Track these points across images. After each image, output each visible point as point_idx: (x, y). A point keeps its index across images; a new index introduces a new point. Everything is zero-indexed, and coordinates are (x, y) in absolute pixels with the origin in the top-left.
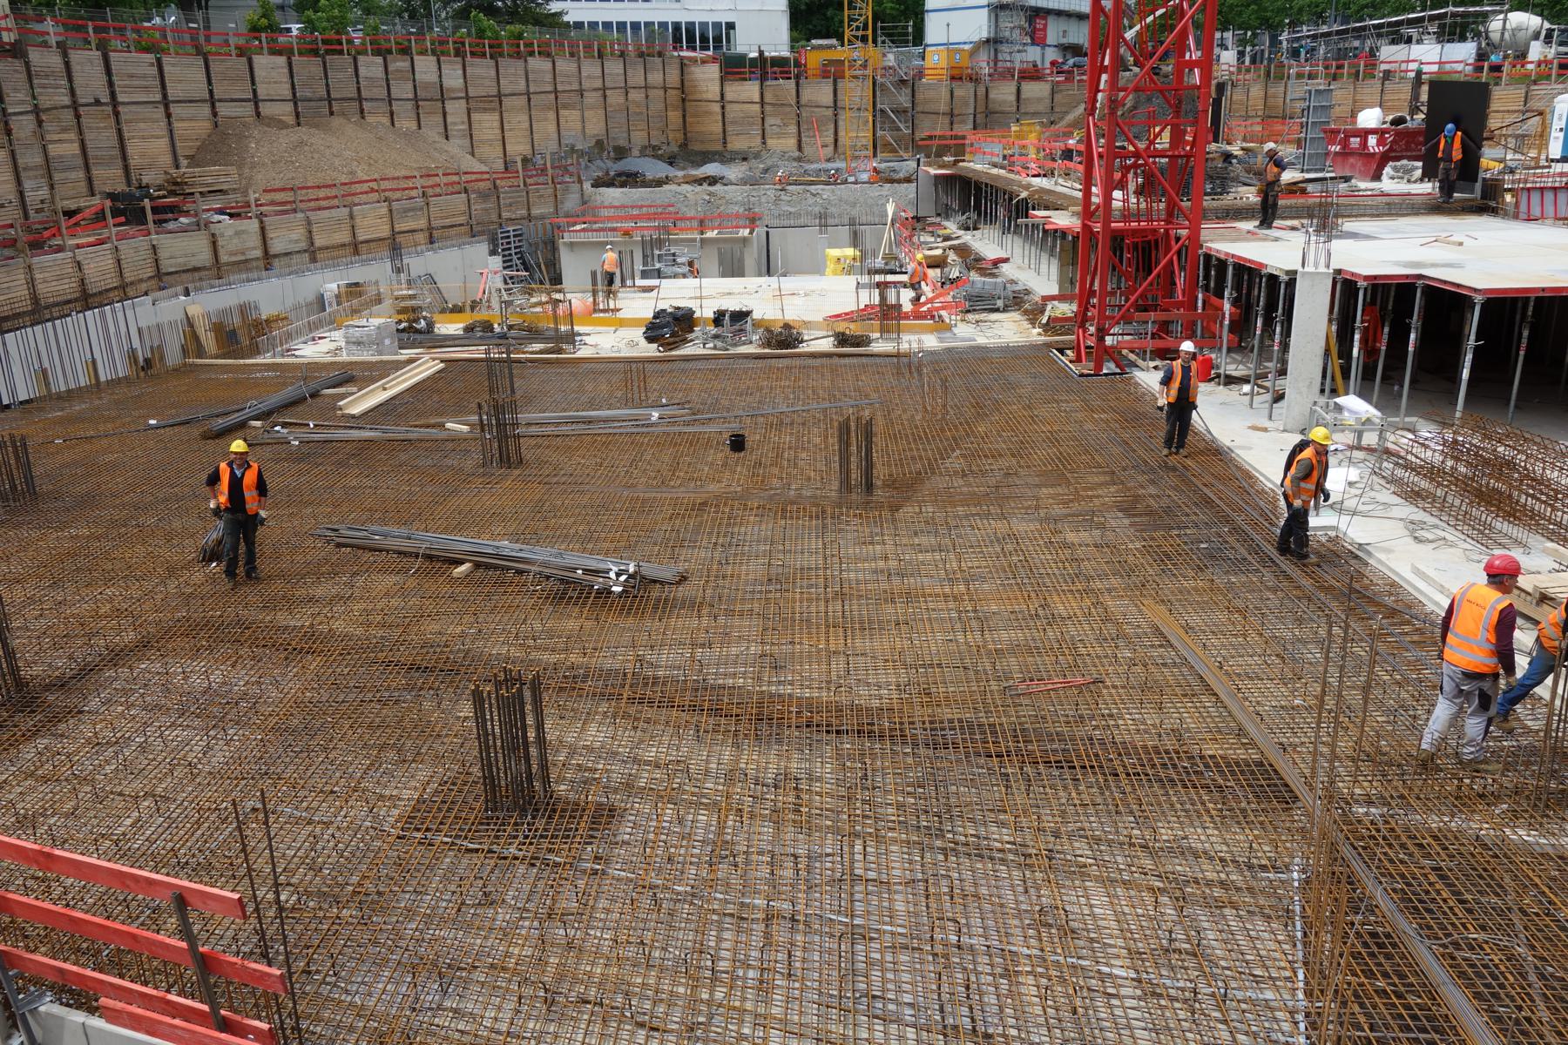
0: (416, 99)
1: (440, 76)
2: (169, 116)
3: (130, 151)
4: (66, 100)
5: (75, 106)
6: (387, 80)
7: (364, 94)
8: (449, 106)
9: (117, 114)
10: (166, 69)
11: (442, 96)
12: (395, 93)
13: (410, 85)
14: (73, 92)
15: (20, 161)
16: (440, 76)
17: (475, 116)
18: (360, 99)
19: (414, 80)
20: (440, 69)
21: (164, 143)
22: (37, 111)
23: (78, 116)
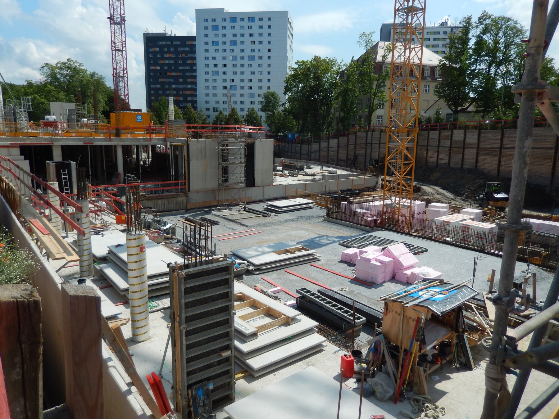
0: (451, 147)
1: (465, 138)
2: (379, 147)
3: (373, 154)
4: (364, 142)
5: (366, 144)
6: (439, 139)
7: (430, 144)
8: (467, 151)
9: (371, 145)
10: (382, 136)
11: (464, 145)
12: (442, 143)
13: (449, 141)
14: (366, 141)
15: (349, 153)
16: (465, 138)
17: (481, 157)
18: (428, 146)
19: (451, 140)
20: (465, 135)
21: (377, 153)
22: (355, 144)
23: (366, 146)
